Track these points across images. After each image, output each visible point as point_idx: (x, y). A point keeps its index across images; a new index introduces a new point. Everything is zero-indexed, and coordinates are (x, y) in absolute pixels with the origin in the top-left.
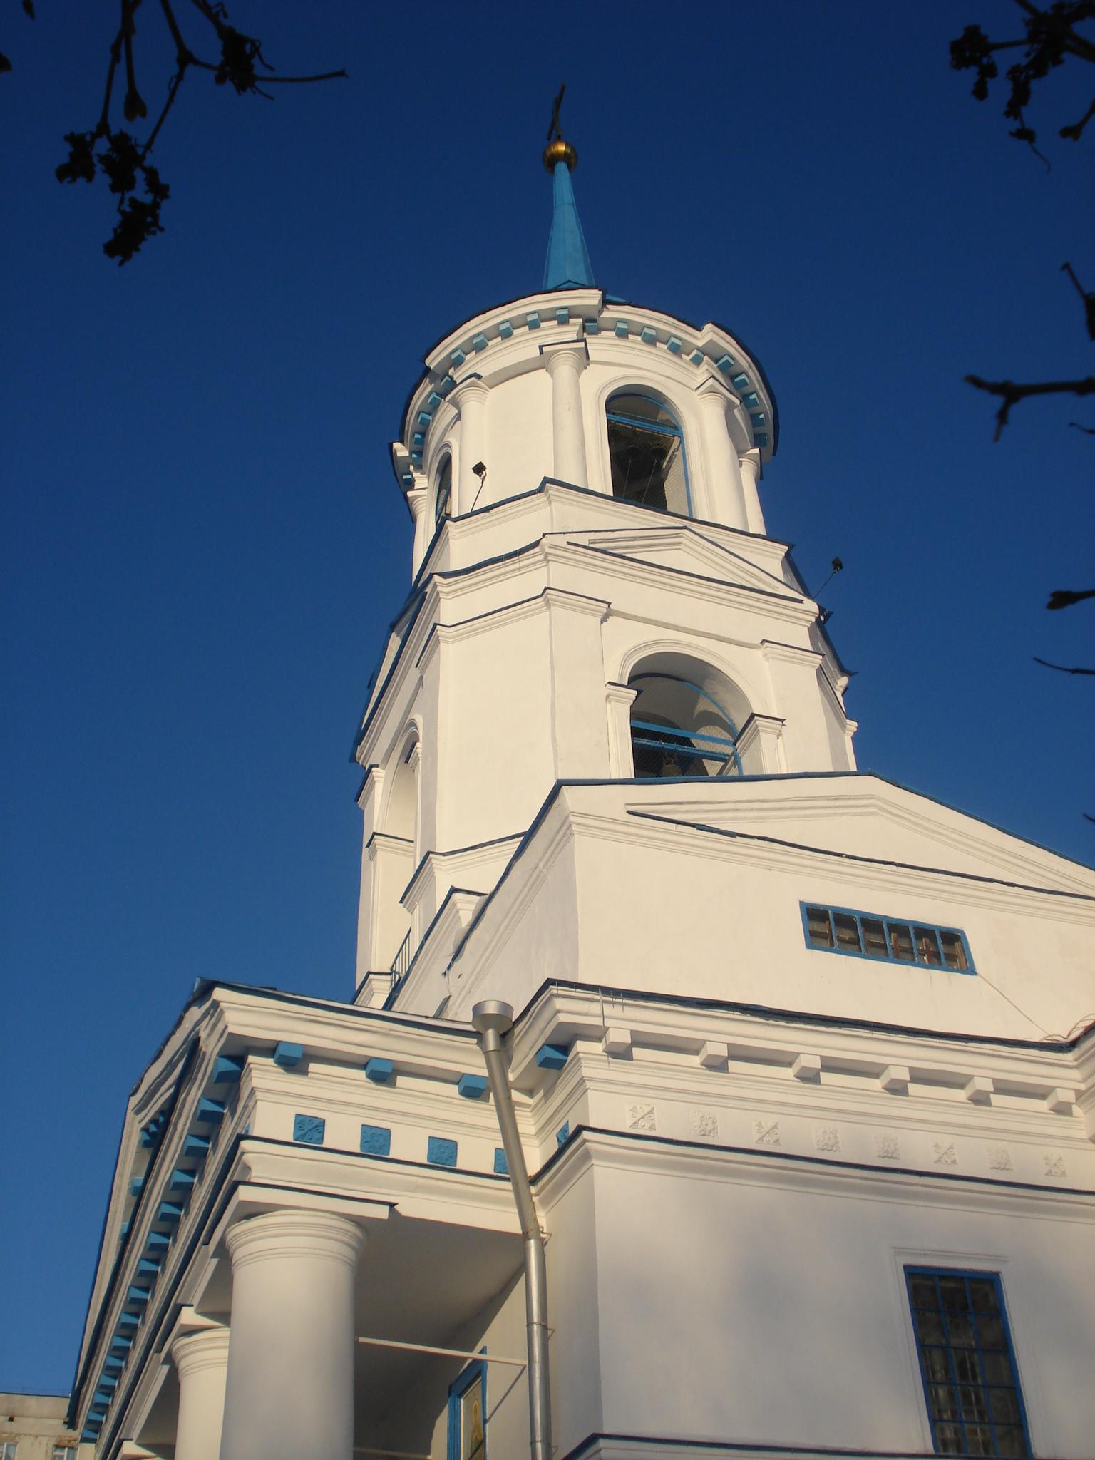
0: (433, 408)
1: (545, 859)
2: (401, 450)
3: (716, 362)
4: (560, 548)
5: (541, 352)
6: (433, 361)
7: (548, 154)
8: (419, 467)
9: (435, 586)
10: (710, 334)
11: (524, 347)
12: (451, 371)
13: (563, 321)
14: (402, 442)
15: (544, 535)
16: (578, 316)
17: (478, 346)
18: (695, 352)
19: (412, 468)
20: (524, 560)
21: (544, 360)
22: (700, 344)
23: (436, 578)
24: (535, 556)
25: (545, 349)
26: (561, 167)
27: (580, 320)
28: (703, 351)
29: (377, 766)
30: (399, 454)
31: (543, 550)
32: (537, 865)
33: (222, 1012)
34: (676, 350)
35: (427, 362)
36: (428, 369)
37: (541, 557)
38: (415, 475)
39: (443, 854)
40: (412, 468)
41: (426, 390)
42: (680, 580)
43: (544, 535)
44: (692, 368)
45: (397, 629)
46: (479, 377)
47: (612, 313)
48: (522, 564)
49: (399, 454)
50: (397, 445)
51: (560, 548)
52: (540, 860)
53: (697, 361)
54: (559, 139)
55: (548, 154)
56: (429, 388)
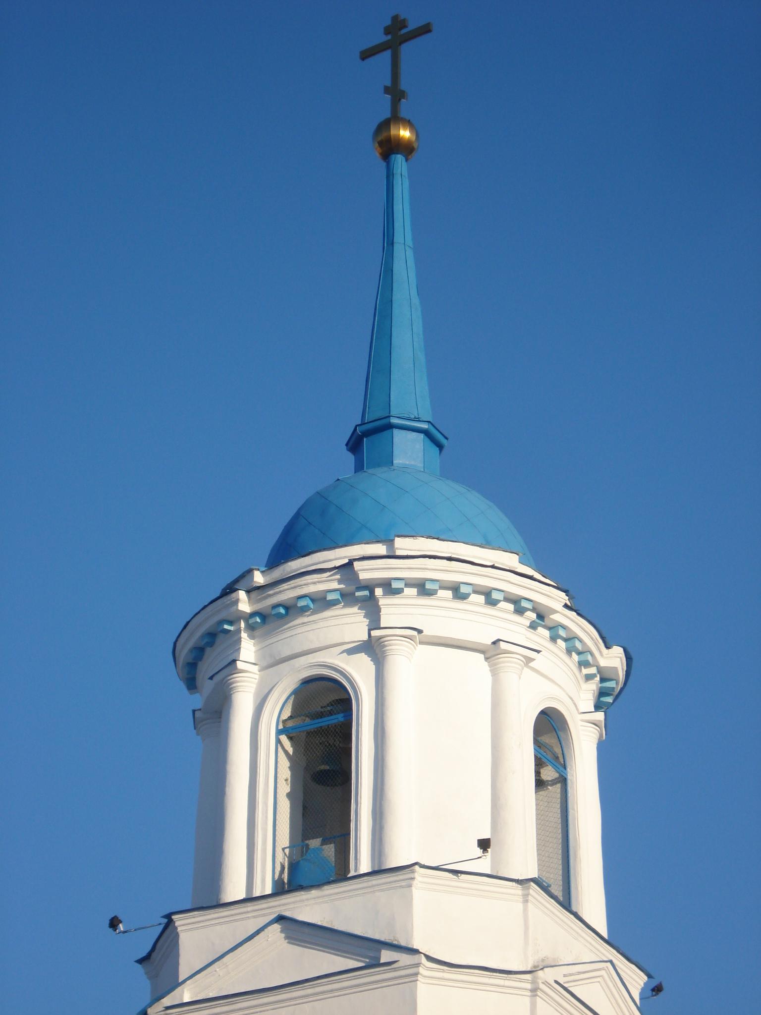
0: (321, 602)
2: (244, 603)
3: (603, 680)
5: (494, 643)
8: (251, 628)
9: (418, 965)
10: (613, 659)
12: (379, 592)
13: (520, 611)
18: (593, 670)
21: (492, 651)
22: (603, 663)
23: (424, 960)
25: (503, 645)
28: (600, 670)
31: (534, 982)
34: (583, 664)
37: (529, 986)
38: (244, 635)
40: (243, 625)
44: (582, 681)
46: (420, 631)
48: (507, 983)
50: (242, 594)
53: (589, 678)
54: (409, 123)
55: (393, 132)
56: (335, 585)
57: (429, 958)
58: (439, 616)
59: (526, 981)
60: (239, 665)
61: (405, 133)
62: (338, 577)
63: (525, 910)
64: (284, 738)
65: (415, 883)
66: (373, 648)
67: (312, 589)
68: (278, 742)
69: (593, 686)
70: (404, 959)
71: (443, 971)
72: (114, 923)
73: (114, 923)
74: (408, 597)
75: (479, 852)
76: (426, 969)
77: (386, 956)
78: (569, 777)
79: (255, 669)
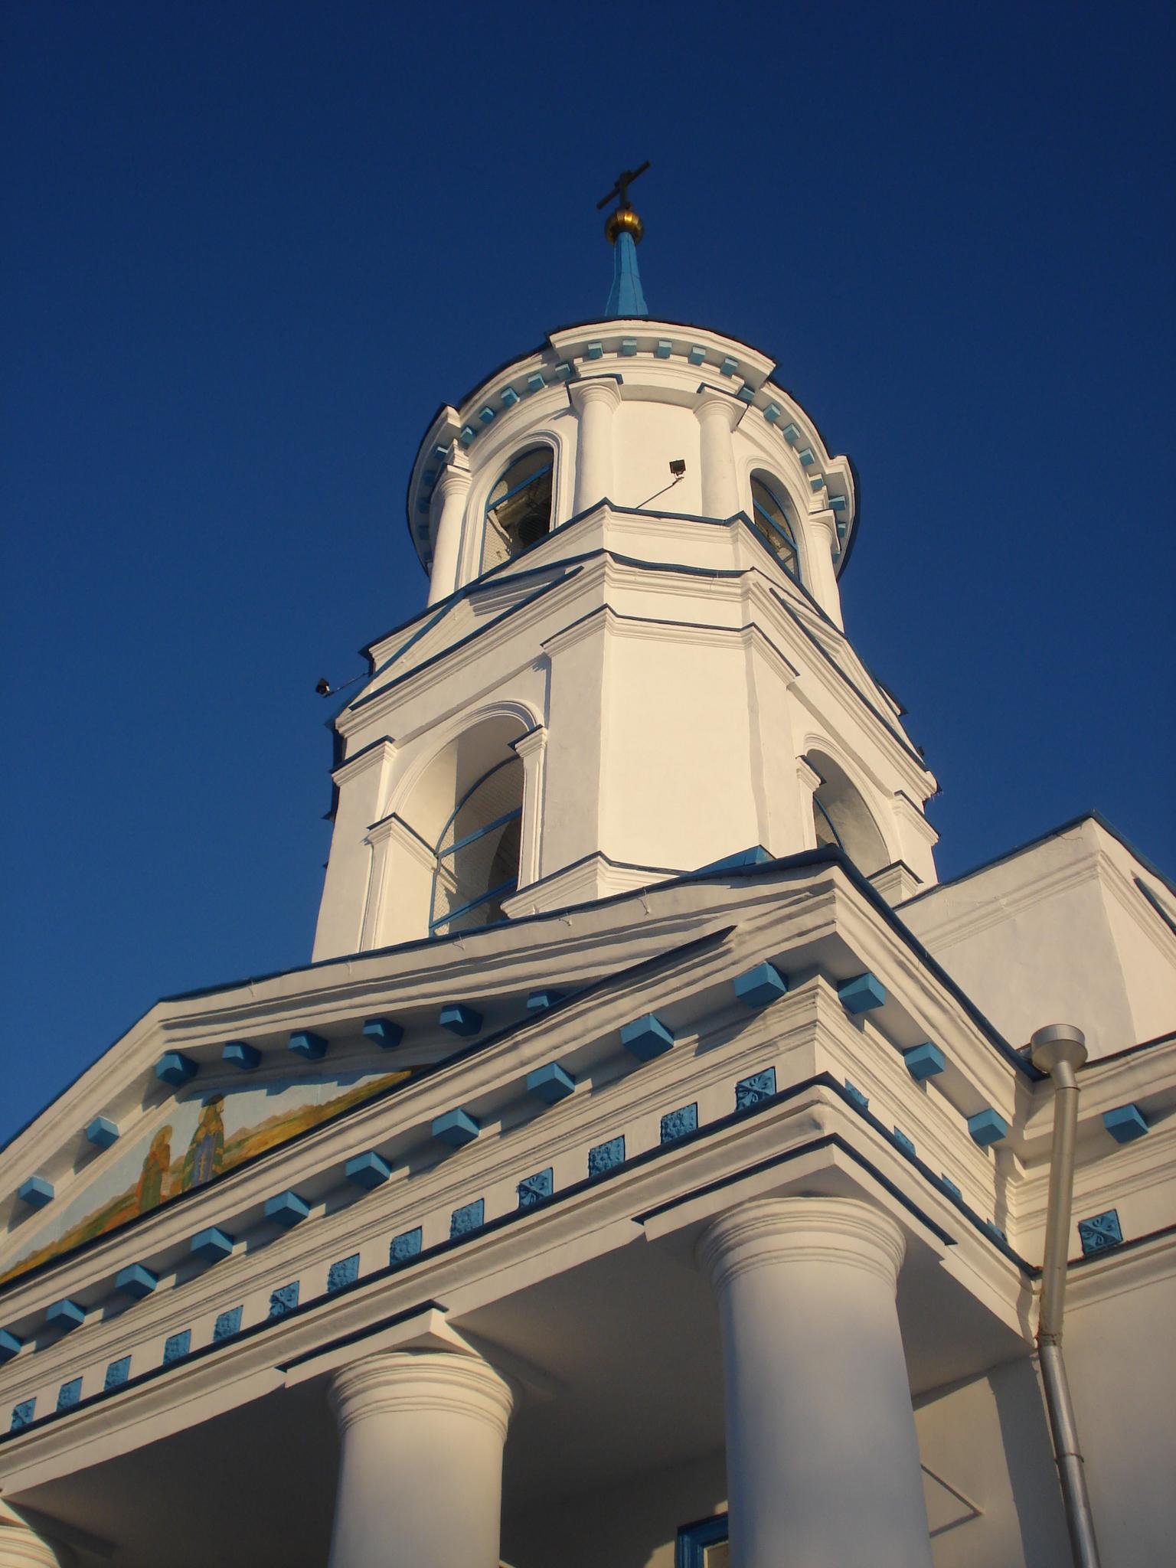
1: (1016, 896)
2: (454, 418)
4: (763, 591)
5: (699, 391)
6: (562, 340)
7: (619, 218)
8: (465, 446)
9: (604, 564)
10: (839, 466)
11: (681, 377)
12: (577, 361)
14: (458, 410)
15: (753, 569)
16: (742, 377)
17: (625, 350)
18: (819, 477)
19: (455, 442)
20: (717, 585)
24: (734, 586)
26: (626, 238)
27: (742, 382)
29: (391, 740)
30: (450, 421)
32: (996, 899)
33: (832, 900)
35: (553, 338)
36: (546, 347)
37: (739, 591)
38: (457, 452)
39: (610, 863)
40: (455, 442)
41: (533, 365)
42: (841, 685)
43: (753, 569)
45: (475, 597)
46: (619, 379)
47: (771, 392)
48: (713, 588)
49: (450, 421)
50: (450, 410)
51: (763, 591)
52: (1005, 895)
53: (816, 487)
55: (619, 218)
57: (617, 558)
58: (640, 372)
59: (735, 585)
60: (450, 468)
61: (628, 219)
62: (540, 357)
63: (736, 550)
64: (492, 514)
65: (605, 521)
66: (576, 408)
67: (514, 377)
68: (487, 517)
69: (821, 495)
70: (588, 565)
71: (635, 574)
72: (321, 688)
73: (321, 688)
74: (608, 361)
75: (673, 477)
76: (613, 569)
77: (569, 570)
78: (800, 551)
79: (468, 475)
